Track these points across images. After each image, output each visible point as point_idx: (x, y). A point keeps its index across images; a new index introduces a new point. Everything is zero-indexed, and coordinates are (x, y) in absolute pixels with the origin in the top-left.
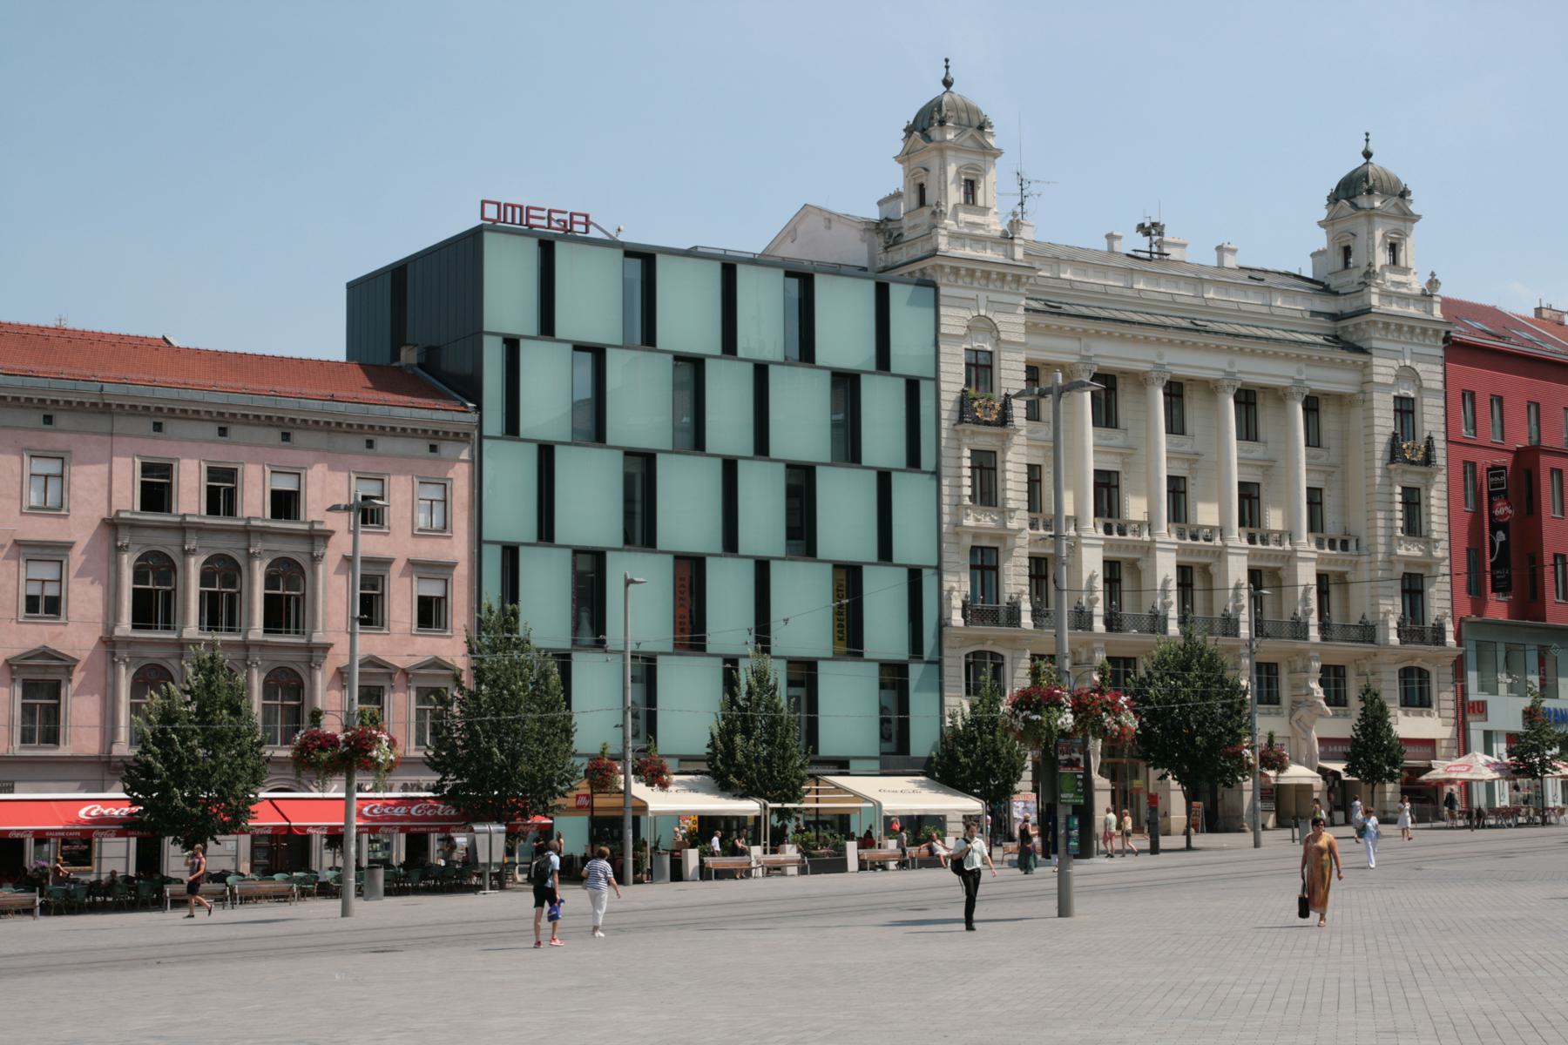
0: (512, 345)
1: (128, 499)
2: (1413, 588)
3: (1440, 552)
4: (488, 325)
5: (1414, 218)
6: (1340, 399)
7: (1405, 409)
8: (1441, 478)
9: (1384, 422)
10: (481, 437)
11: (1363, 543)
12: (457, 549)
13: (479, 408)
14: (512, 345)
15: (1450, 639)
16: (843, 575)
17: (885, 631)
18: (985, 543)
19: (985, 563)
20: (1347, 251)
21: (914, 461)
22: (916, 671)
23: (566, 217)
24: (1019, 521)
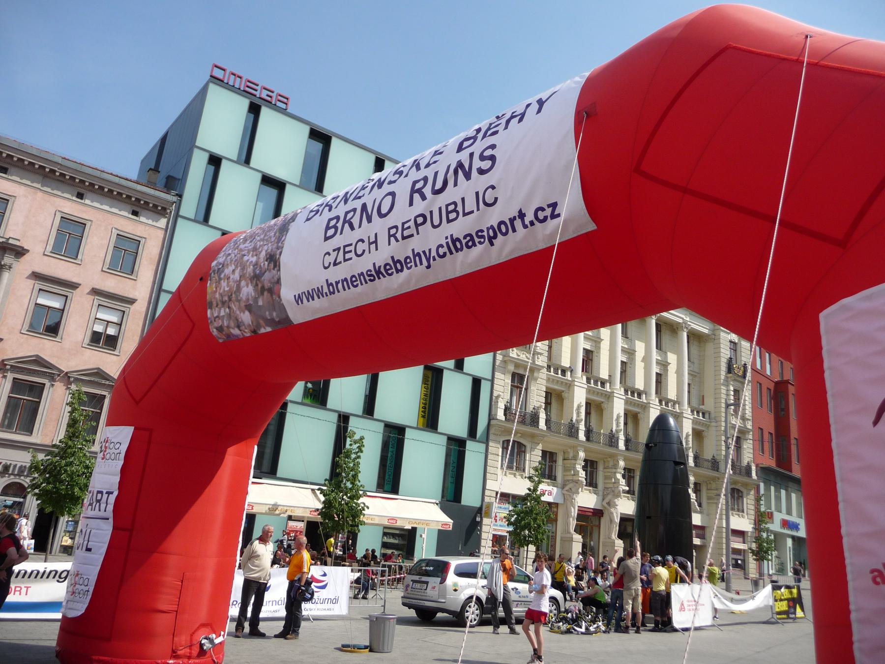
10: (177, 216)
11: (713, 416)
22: (470, 445)
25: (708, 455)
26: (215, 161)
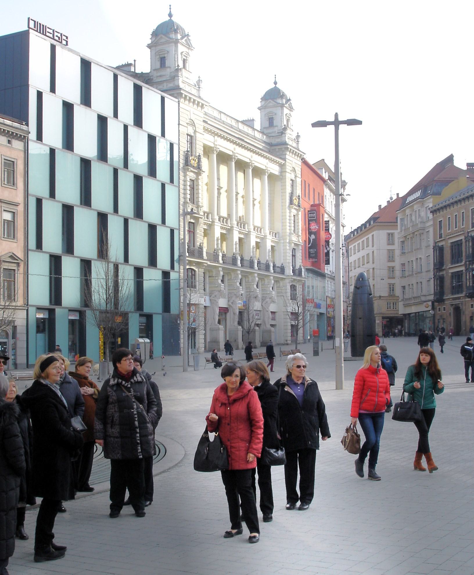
0: (40, 95)
4: (32, 81)
9: (289, 190)
13: (27, 124)
14: (40, 95)
21: (172, 181)
23: (59, 35)
25: (278, 264)
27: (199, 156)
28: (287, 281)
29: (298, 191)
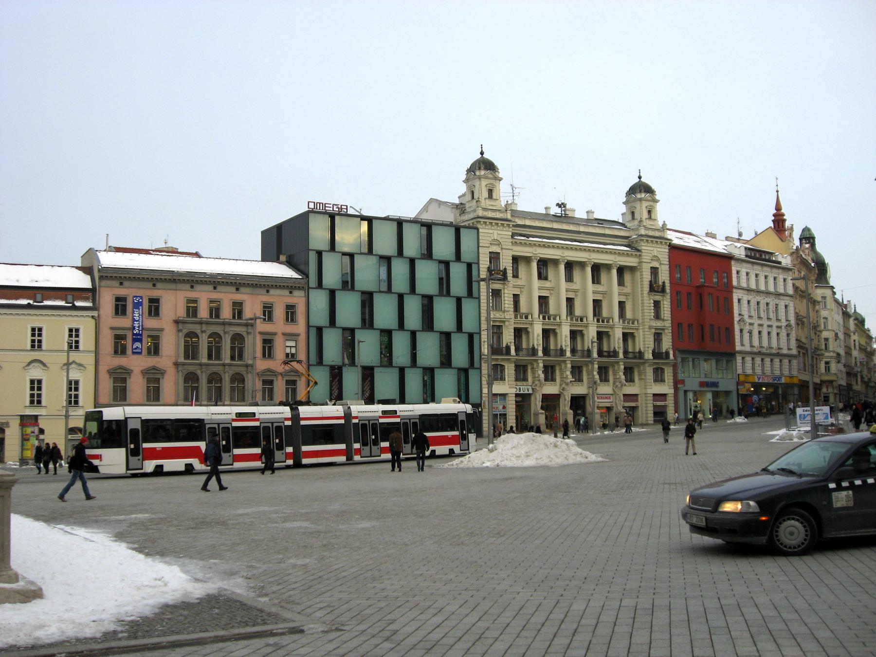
0: (319, 254)
1: (182, 313)
2: (658, 337)
3: (668, 324)
5: (657, 201)
6: (632, 269)
7: (654, 271)
8: (668, 297)
9: (647, 276)
11: (640, 321)
12: (300, 327)
15: (671, 356)
16: (443, 338)
17: (460, 357)
18: (498, 324)
19: (497, 330)
20: (633, 213)
22: (471, 372)
24: (510, 315)
26: (319, 254)
27: (505, 269)
28: (647, 365)
29: (664, 276)
